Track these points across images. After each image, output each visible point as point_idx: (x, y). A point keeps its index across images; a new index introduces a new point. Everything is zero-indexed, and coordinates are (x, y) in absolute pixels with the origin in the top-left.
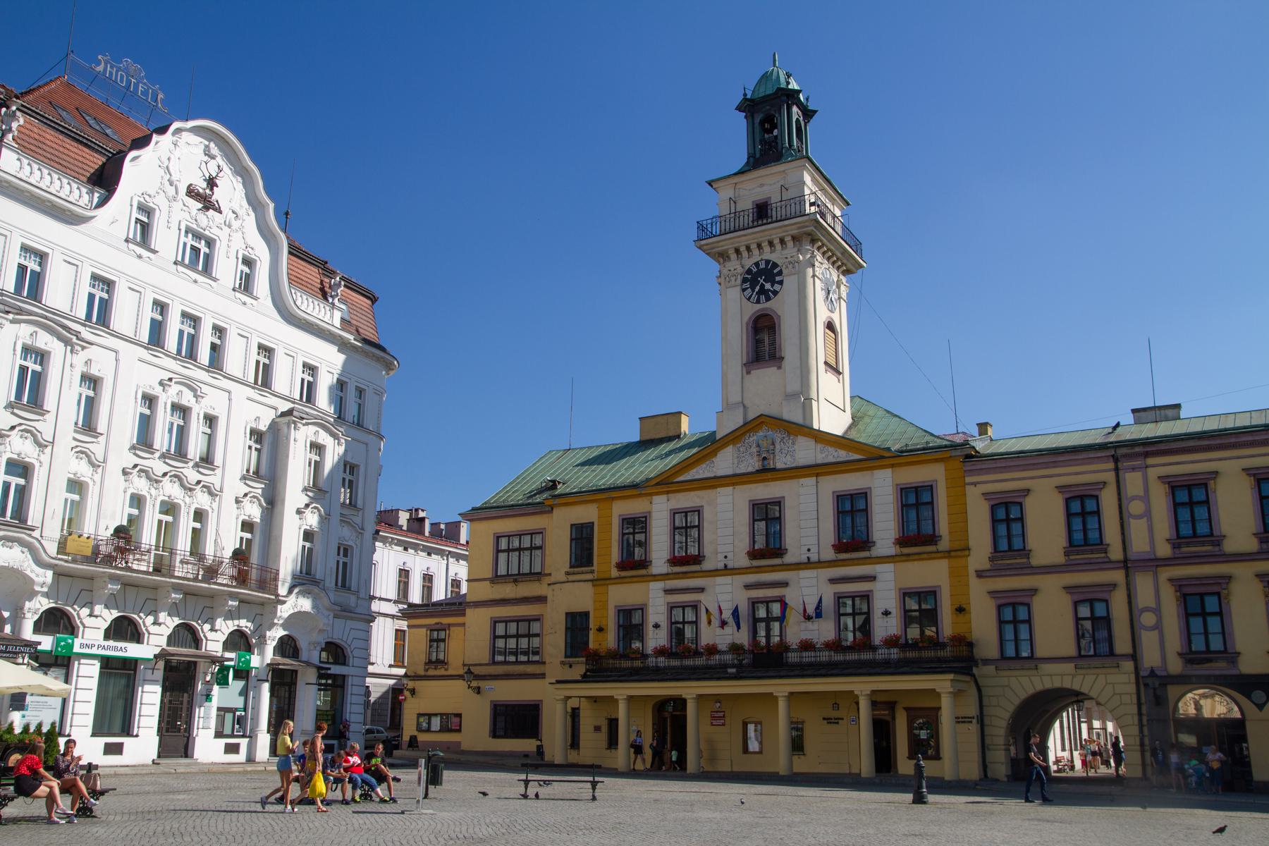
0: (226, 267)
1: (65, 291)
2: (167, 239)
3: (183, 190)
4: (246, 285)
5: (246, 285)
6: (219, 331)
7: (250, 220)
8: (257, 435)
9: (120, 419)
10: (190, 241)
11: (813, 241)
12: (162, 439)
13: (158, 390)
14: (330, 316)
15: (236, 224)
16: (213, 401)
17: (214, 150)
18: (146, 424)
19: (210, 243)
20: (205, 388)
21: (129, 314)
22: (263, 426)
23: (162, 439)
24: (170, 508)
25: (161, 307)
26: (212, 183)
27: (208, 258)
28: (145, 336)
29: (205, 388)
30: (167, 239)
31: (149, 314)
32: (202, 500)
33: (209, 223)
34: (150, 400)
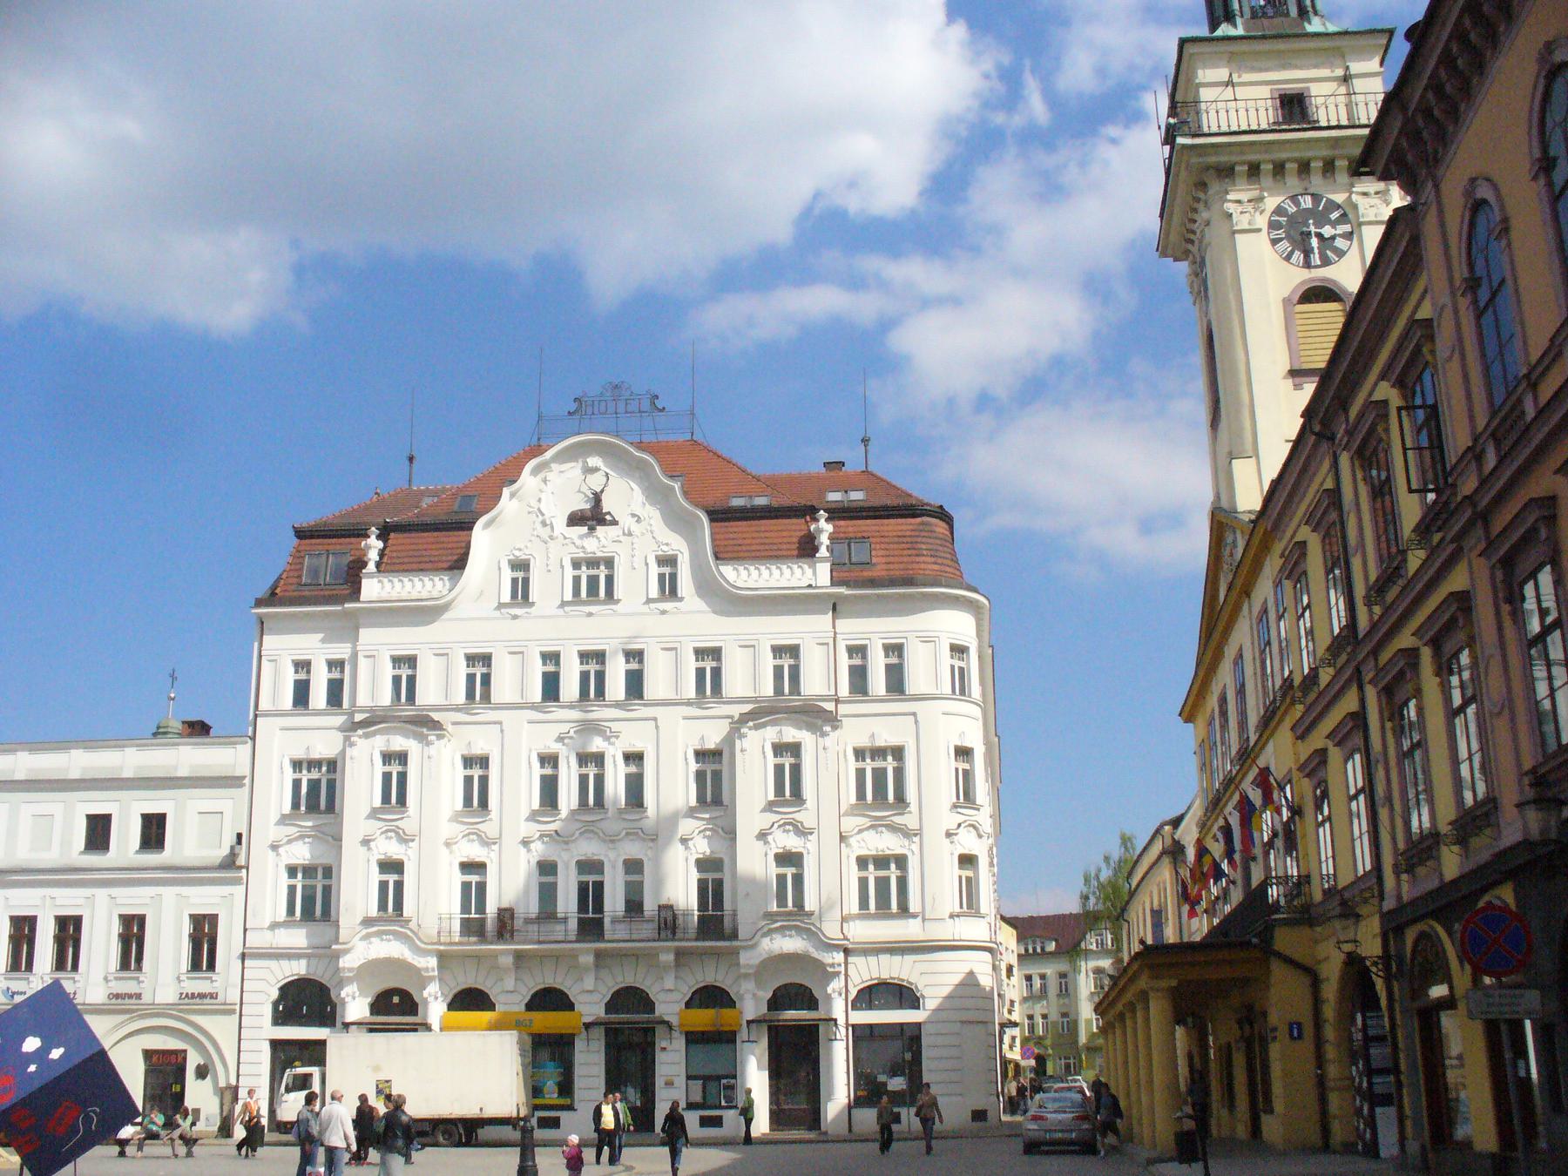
0: (635, 580)
1: (439, 685)
2: (551, 584)
3: (560, 523)
4: (669, 588)
5: (669, 588)
6: (635, 655)
7: (653, 515)
8: (701, 755)
9: (516, 790)
10: (584, 573)
11: (1226, 173)
12: (568, 797)
13: (555, 747)
14: (818, 575)
15: (635, 528)
16: (633, 735)
17: (594, 461)
18: (549, 789)
19: (609, 563)
20: (615, 726)
21: (515, 679)
22: (711, 745)
23: (568, 797)
24: (589, 866)
25: (552, 657)
26: (597, 498)
27: (610, 580)
28: (536, 694)
29: (615, 726)
30: (551, 584)
31: (537, 670)
32: (633, 850)
33: (601, 541)
34: (549, 760)
